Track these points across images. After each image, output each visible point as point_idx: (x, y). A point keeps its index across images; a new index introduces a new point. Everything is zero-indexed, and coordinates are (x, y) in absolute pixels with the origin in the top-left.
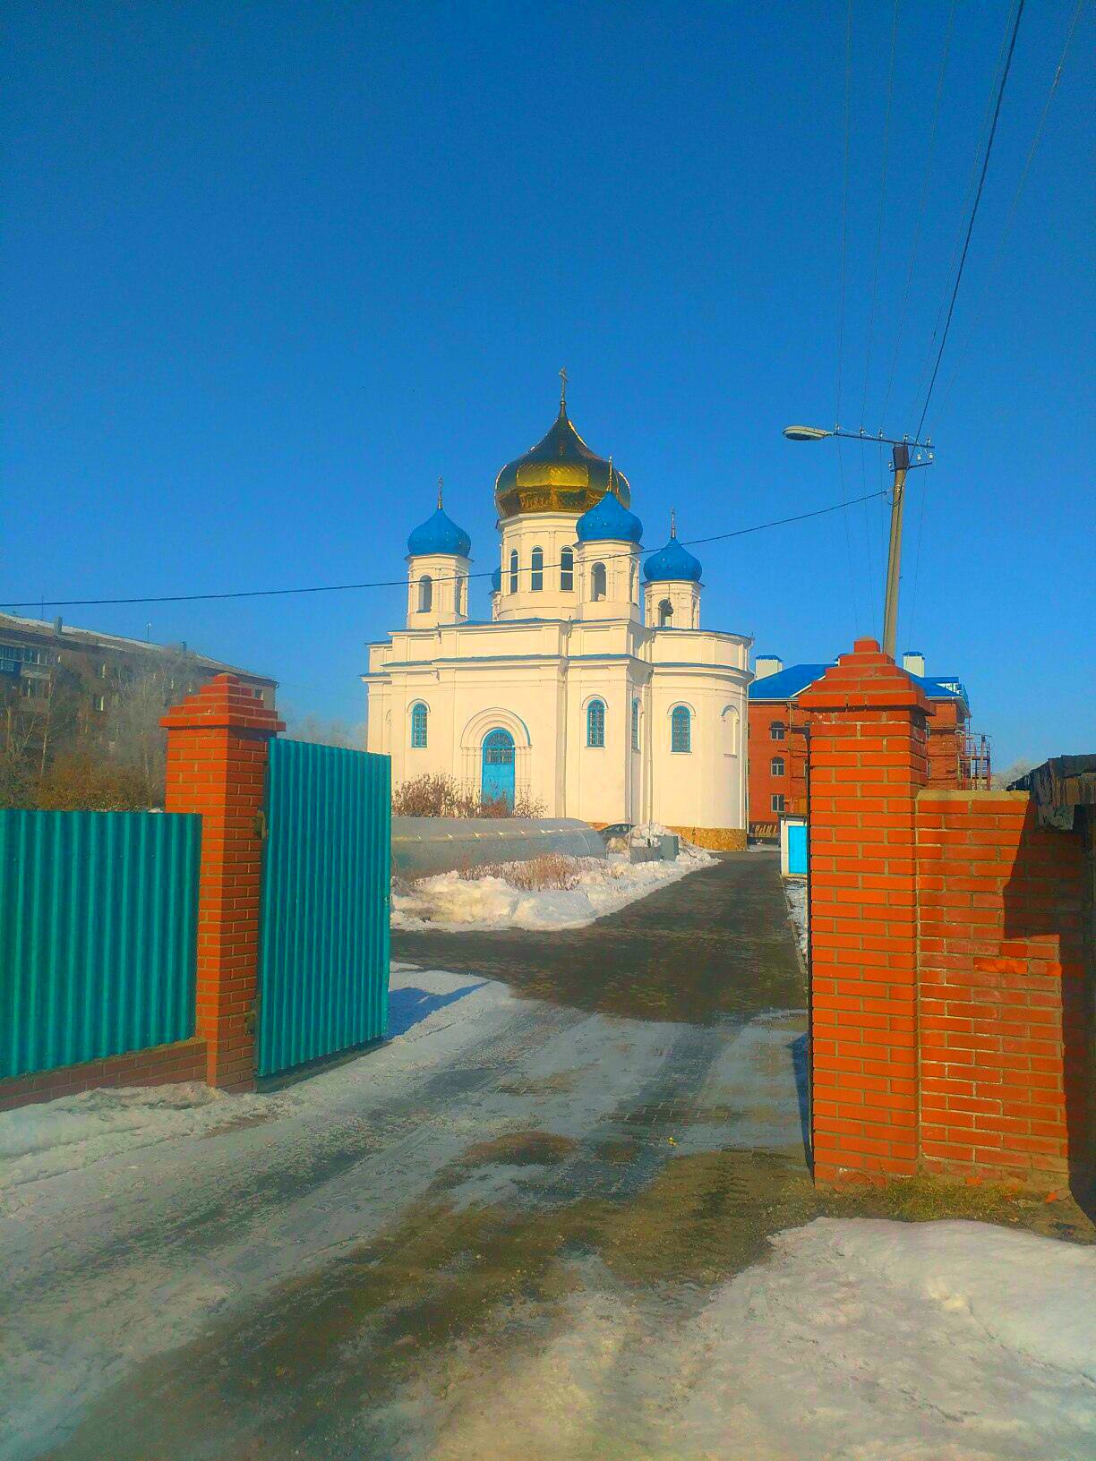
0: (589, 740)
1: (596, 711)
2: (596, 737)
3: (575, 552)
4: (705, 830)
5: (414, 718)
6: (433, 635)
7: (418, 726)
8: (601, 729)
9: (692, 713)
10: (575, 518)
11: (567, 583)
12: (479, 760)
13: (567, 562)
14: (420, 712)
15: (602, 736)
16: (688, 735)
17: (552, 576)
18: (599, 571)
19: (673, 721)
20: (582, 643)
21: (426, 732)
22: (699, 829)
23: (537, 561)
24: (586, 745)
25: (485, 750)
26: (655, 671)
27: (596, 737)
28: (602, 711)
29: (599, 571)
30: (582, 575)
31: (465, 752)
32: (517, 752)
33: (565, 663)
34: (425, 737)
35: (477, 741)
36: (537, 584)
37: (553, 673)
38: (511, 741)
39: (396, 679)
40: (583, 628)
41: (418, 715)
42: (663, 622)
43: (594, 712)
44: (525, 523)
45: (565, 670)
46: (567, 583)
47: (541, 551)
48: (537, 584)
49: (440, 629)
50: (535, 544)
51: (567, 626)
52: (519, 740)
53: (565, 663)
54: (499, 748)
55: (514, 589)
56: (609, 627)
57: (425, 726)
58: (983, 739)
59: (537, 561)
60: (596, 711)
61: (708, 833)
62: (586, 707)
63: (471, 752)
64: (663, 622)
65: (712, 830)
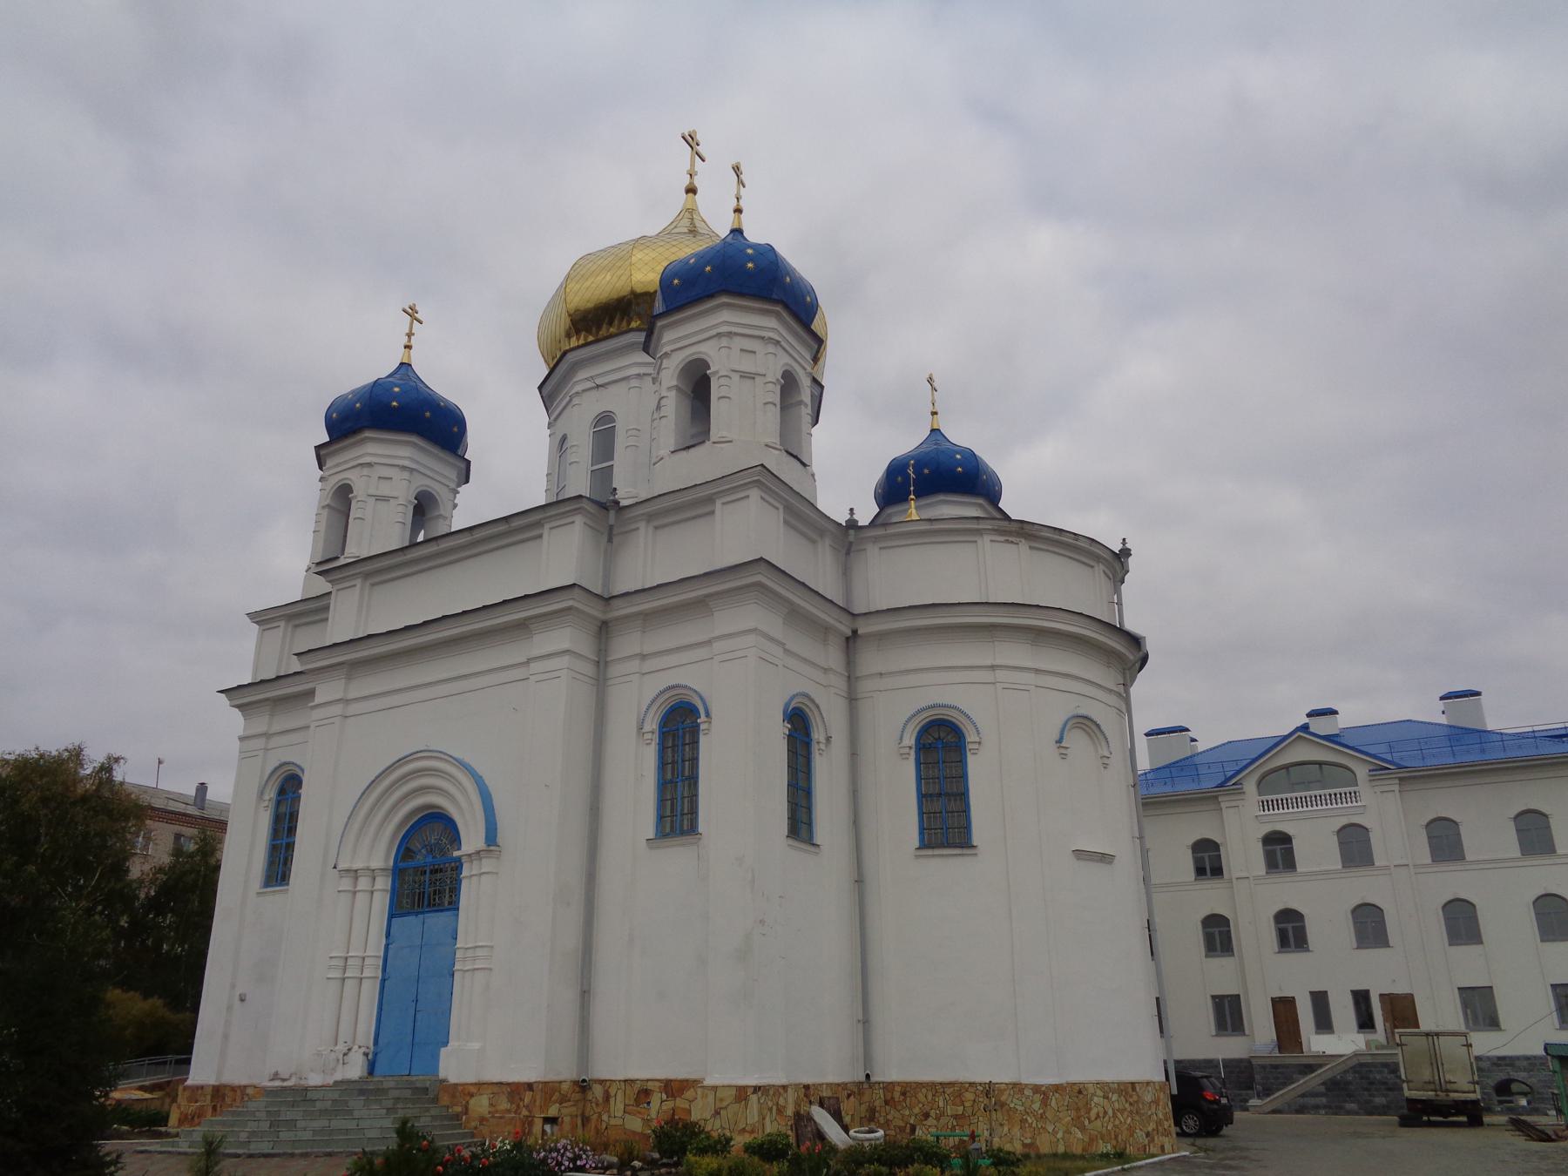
0: (661, 818)
4: (1036, 1089)
8: (693, 780)
9: (971, 737)
12: (381, 902)
16: (963, 796)
19: (918, 763)
22: (1017, 1087)
24: (650, 832)
25: (398, 873)
26: (859, 632)
28: (695, 731)
31: (346, 884)
37: (563, 638)
38: (456, 839)
40: (650, 517)
45: (604, 631)
47: (614, 421)
50: (599, 408)
62: (652, 725)
63: (364, 883)
65: (1057, 1088)
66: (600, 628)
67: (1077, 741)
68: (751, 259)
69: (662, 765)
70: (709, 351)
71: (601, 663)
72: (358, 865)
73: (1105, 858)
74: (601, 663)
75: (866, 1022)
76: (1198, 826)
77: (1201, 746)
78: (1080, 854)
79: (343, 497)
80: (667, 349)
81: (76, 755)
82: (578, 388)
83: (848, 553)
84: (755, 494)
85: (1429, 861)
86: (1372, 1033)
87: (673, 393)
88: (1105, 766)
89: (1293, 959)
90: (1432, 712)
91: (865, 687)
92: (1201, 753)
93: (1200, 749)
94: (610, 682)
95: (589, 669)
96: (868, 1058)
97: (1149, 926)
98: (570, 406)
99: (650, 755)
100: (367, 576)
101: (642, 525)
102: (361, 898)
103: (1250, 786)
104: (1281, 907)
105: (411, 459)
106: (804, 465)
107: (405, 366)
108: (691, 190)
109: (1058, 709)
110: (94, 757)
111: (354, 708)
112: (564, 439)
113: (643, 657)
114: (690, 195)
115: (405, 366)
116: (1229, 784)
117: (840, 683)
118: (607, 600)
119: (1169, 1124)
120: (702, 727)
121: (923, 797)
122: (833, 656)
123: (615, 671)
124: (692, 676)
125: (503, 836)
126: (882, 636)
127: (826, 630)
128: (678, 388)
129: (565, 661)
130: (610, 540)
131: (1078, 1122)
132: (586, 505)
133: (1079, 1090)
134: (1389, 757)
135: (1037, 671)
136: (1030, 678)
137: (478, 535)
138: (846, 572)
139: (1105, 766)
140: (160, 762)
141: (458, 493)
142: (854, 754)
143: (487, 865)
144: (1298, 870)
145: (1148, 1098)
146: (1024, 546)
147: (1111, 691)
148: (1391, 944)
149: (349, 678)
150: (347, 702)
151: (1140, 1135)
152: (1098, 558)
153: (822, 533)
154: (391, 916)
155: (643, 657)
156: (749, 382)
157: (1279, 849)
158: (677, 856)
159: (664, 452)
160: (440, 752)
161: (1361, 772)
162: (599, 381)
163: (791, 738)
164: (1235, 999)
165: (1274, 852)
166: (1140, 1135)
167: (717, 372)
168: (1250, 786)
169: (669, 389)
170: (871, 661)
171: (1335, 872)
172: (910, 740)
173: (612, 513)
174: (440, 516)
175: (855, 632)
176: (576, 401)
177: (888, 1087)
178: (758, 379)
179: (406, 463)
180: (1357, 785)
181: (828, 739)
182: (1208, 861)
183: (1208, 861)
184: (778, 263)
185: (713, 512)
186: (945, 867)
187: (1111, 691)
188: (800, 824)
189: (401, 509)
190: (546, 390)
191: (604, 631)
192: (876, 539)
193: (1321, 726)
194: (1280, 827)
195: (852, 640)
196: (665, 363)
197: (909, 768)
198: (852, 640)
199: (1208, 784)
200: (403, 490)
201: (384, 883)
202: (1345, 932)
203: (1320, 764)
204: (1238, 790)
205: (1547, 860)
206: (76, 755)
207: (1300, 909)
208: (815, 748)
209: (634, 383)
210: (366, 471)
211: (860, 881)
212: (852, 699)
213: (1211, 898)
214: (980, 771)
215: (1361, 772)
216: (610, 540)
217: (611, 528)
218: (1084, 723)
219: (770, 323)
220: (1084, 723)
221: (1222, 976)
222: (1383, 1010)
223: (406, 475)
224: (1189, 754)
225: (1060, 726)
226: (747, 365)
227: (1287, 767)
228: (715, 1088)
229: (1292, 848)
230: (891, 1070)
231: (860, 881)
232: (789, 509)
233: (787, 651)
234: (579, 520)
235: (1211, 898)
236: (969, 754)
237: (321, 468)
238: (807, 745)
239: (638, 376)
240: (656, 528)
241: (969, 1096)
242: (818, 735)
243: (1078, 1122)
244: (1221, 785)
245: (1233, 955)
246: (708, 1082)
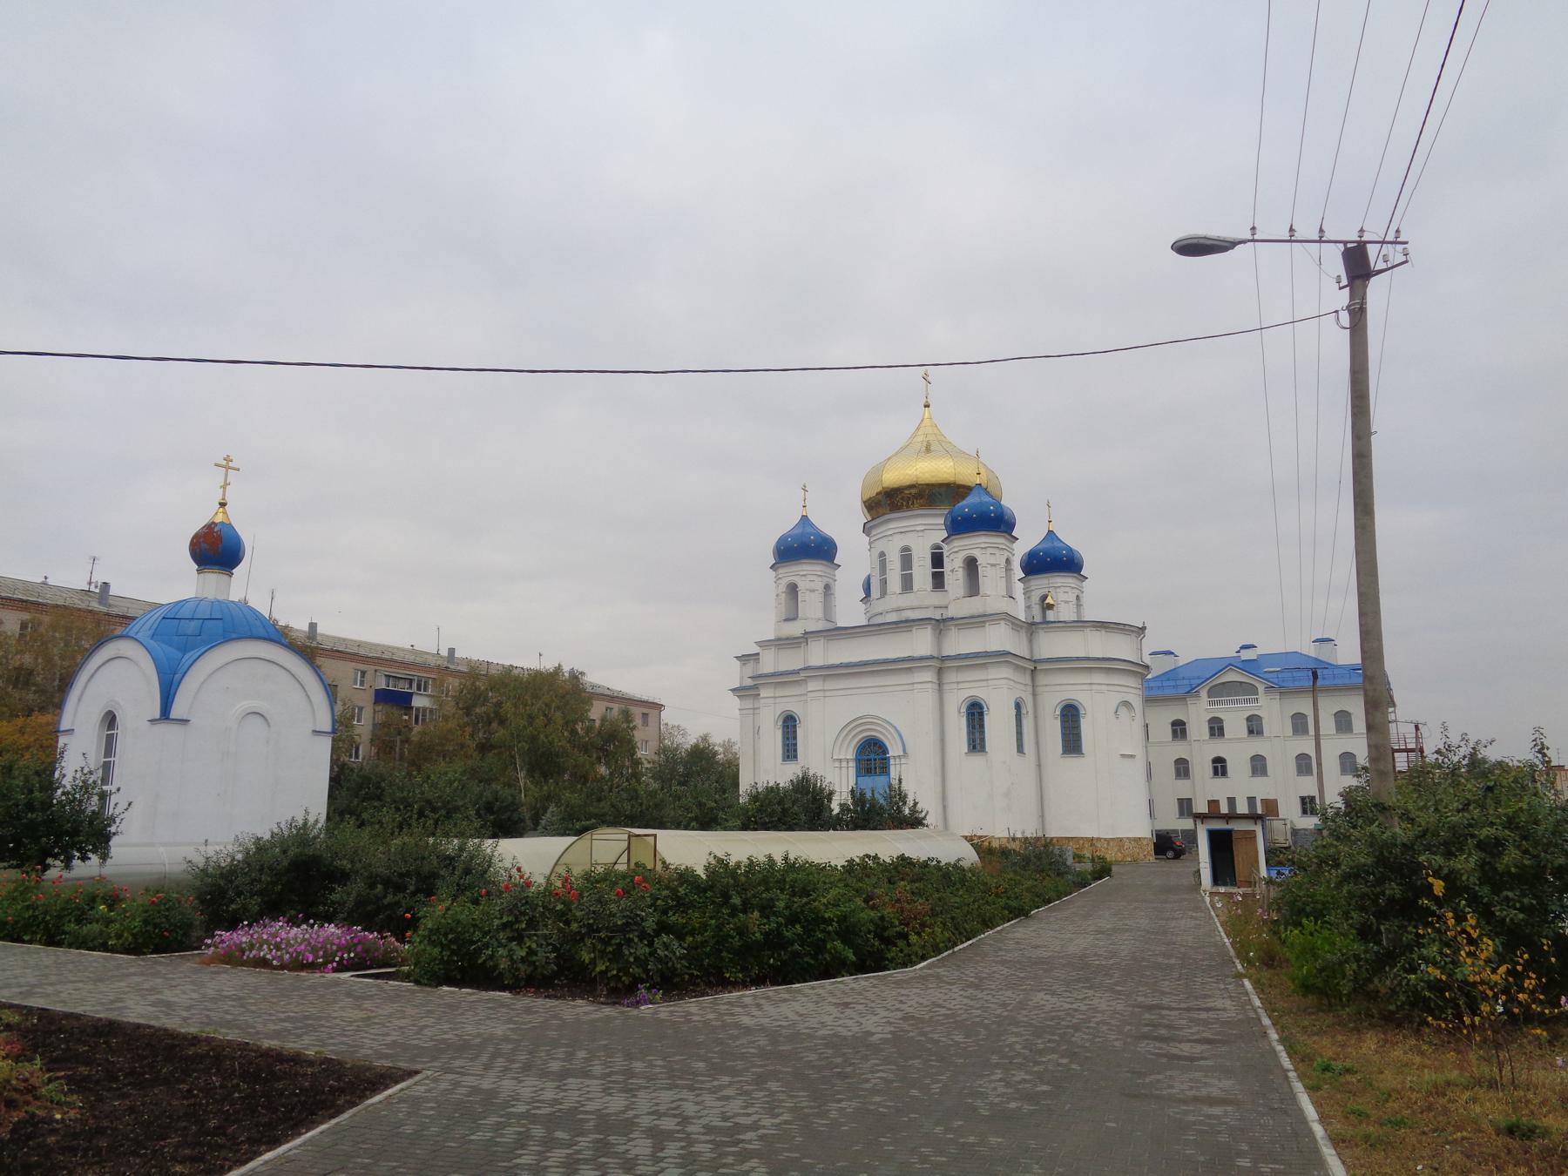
0: (969, 744)
1: (975, 713)
2: (977, 743)
3: (946, 548)
4: (1105, 839)
5: (783, 732)
6: (800, 643)
7: (788, 739)
8: (982, 732)
9: (1082, 712)
10: (941, 515)
11: (938, 581)
12: (852, 772)
13: (937, 560)
14: (789, 724)
15: (983, 740)
17: (922, 571)
18: (971, 565)
20: (961, 643)
21: (796, 744)
22: (1099, 839)
23: (907, 559)
24: (966, 751)
25: (858, 760)
27: (977, 743)
28: (981, 714)
29: (971, 565)
30: (952, 571)
31: (837, 764)
32: (892, 762)
33: (942, 665)
34: (795, 750)
35: (849, 753)
36: (907, 583)
37: (929, 676)
39: (764, 693)
40: (956, 625)
41: (788, 727)
42: (1044, 616)
43: (973, 714)
44: (892, 525)
46: (938, 581)
48: (907, 583)
49: (807, 636)
50: (902, 544)
51: (941, 625)
52: (894, 750)
53: (942, 665)
54: (872, 755)
55: (884, 593)
56: (984, 622)
57: (795, 738)
58: (1417, 728)
59: (907, 559)
60: (975, 713)
61: (1108, 844)
62: (964, 710)
63: (844, 764)
64: (1044, 616)
65: (1113, 839)
67: (1123, 711)
68: (992, 512)
69: (968, 726)
71: (940, 684)
72: (841, 757)
73: (1132, 756)
74: (940, 684)
75: (1042, 816)
76: (1176, 713)
77: (1182, 661)
78: (1123, 756)
79: (793, 589)
81: (559, 669)
83: (1031, 635)
84: (1002, 622)
85: (1291, 734)
86: (1160, 831)
87: (961, 569)
88: (1133, 720)
89: (1220, 781)
90: (1310, 650)
91: (1039, 690)
92: (1181, 666)
93: (1181, 664)
95: (936, 687)
96: (1043, 829)
97: (1150, 802)
99: (964, 721)
100: (825, 637)
102: (844, 770)
103: (1204, 694)
104: (1216, 755)
105: (825, 572)
107: (805, 518)
109: (1116, 699)
110: (566, 668)
111: (828, 694)
112: (882, 554)
113: (958, 683)
115: (805, 518)
116: (1192, 692)
117: (1030, 689)
118: (944, 659)
119: (1153, 852)
121: (1063, 734)
122: (1028, 681)
123: (945, 687)
125: (909, 750)
126: (1046, 670)
127: (1025, 668)
128: (963, 568)
129: (930, 685)
131: (1119, 850)
132: (933, 622)
133: (1121, 840)
134: (1276, 681)
135: (1108, 685)
136: (1104, 687)
137: (882, 627)
138: (1030, 641)
139: (1133, 720)
140: (540, 655)
141: (835, 580)
142: (1036, 717)
143: (903, 761)
144: (1226, 736)
145: (1145, 843)
146: (1103, 632)
147: (1136, 688)
148: (1269, 774)
149: (824, 680)
150: (824, 690)
151: (1141, 855)
152: (1133, 631)
153: (1022, 627)
154: (857, 776)
155: (958, 683)
157: (1216, 728)
158: (977, 760)
160: (888, 722)
161: (1261, 688)
162: (902, 530)
163: (1016, 715)
164: (1189, 800)
165: (1214, 727)
166: (1141, 855)
168: (1204, 694)
170: (1042, 680)
171: (1244, 738)
172: (1058, 712)
173: (942, 627)
174: (831, 594)
175: (1035, 668)
177: (1052, 839)
179: (819, 573)
180: (1257, 694)
181: (1027, 712)
182: (1179, 729)
183: (1179, 729)
184: (1003, 513)
186: (1072, 762)
187: (1136, 688)
188: (1020, 748)
189: (821, 595)
190: (867, 526)
191: (940, 671)
192: (1043, 629)
193: (1248, 655)
194: (1217, 715)
195: (1034, 671)
197: (1058, 723)
198: (1034, 671)
199: (1182, 691)
200: (820, 586)
201: (852, 764)
202: (1248, 768)
203: (1241, 682)
204: (1198, 696)
205: (1349, 736)
206: (559, 669)
207: (1224, 757)
208: (1022, 716)
209: (921, 534)
210: (803, 578)
211: (1039, 766)
212: (1034, 695)
213: (1179, 750)
214: (1085, 724)
215: (1261, 688)
218: (1126, 704)
219: (1000, 540)
220: (1126, 704)
221: (1183, 789)
222: (1262, 806)
223: (820, 579)
224: (1174, 667)
225: (1115, 706)
227: (1224, 683)
228: (999, 838)
229: (1223, 726)
230: (1053, 833)
231: (1039, 766)
232: (1013, 623)
233: (1013, 681)
234: (929, 627)
235: (1179, 750)
236: (1081, 719)
238: (1020, 715)
239: (922, 531)
241: (1081, 842)
242: (1024, 711)
243: (1119, 850)
244: (1188, 692)
245: (1189, 778)
246: (996, 836)
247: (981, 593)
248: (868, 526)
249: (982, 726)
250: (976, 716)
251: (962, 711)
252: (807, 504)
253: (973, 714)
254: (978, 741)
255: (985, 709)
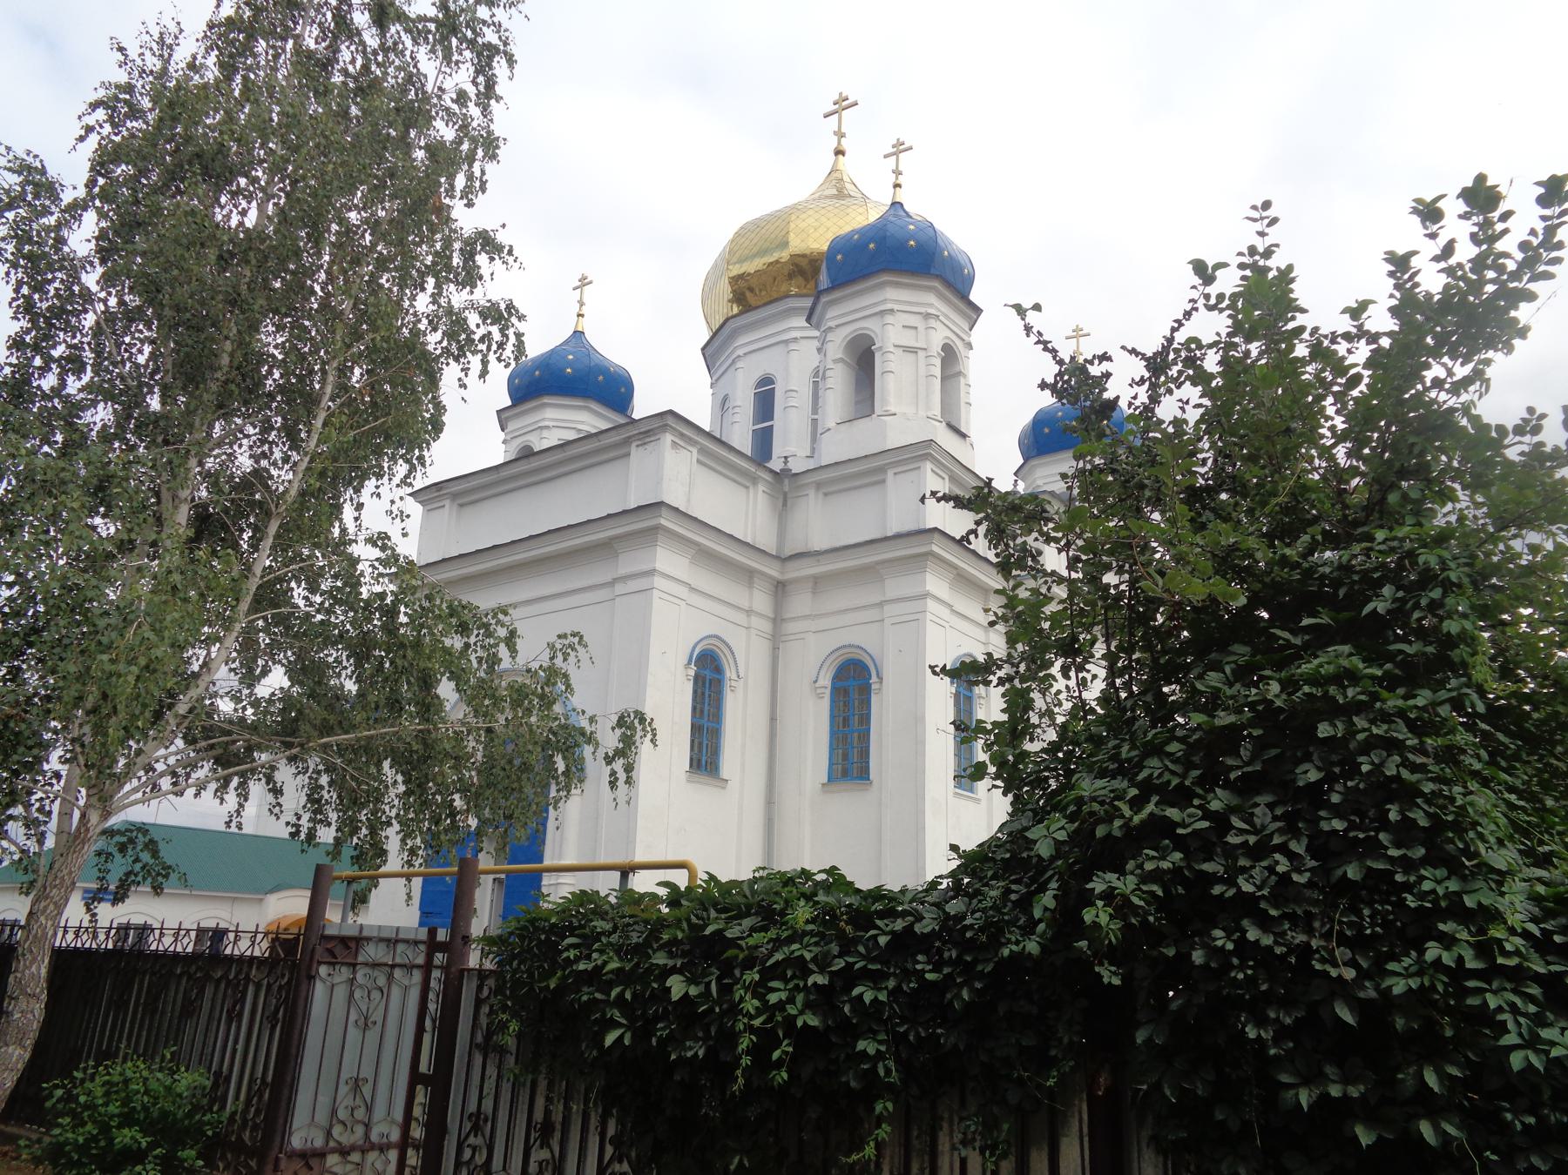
28: (865, 691)
40: (818, 485)
62: (826, 680)
66: (776, 587)
70: (872, 326)
71: (778, 620)
80: (832, 324)
82: (740, 352)
94: (784, 638)
95: (766, 626)
98: (732, 369)
101: (812, 492)
106: (964, 436)
107: (578, 334)
108: (839, 152)
112: (725, 399)
114: (840, 157)
115: (578, 334)
120: (873, 687)
124: (859, 635)
130: (785, 504)
156: (911, 357)
159: (831, 424)
167: (881, 348)
169: (835, 361)
176: (739, 365)
178: (921, 354)
185: (884, 481)
196: (830, 336)
208: (976, 701)
216: (785, 504)
217: (785, 495)
219: (932, 300)
226: (908, 339)
233: (954, 612)
237: (503, 430)
240: (826, 494)
247: (878, 410)
248: (709, 351)
249: (865, 719)
250: (855, 695)
251: (821, 682)
252: (585, 310)
253: (846, 692)
254: (855, 755)
255: (874, 679)
